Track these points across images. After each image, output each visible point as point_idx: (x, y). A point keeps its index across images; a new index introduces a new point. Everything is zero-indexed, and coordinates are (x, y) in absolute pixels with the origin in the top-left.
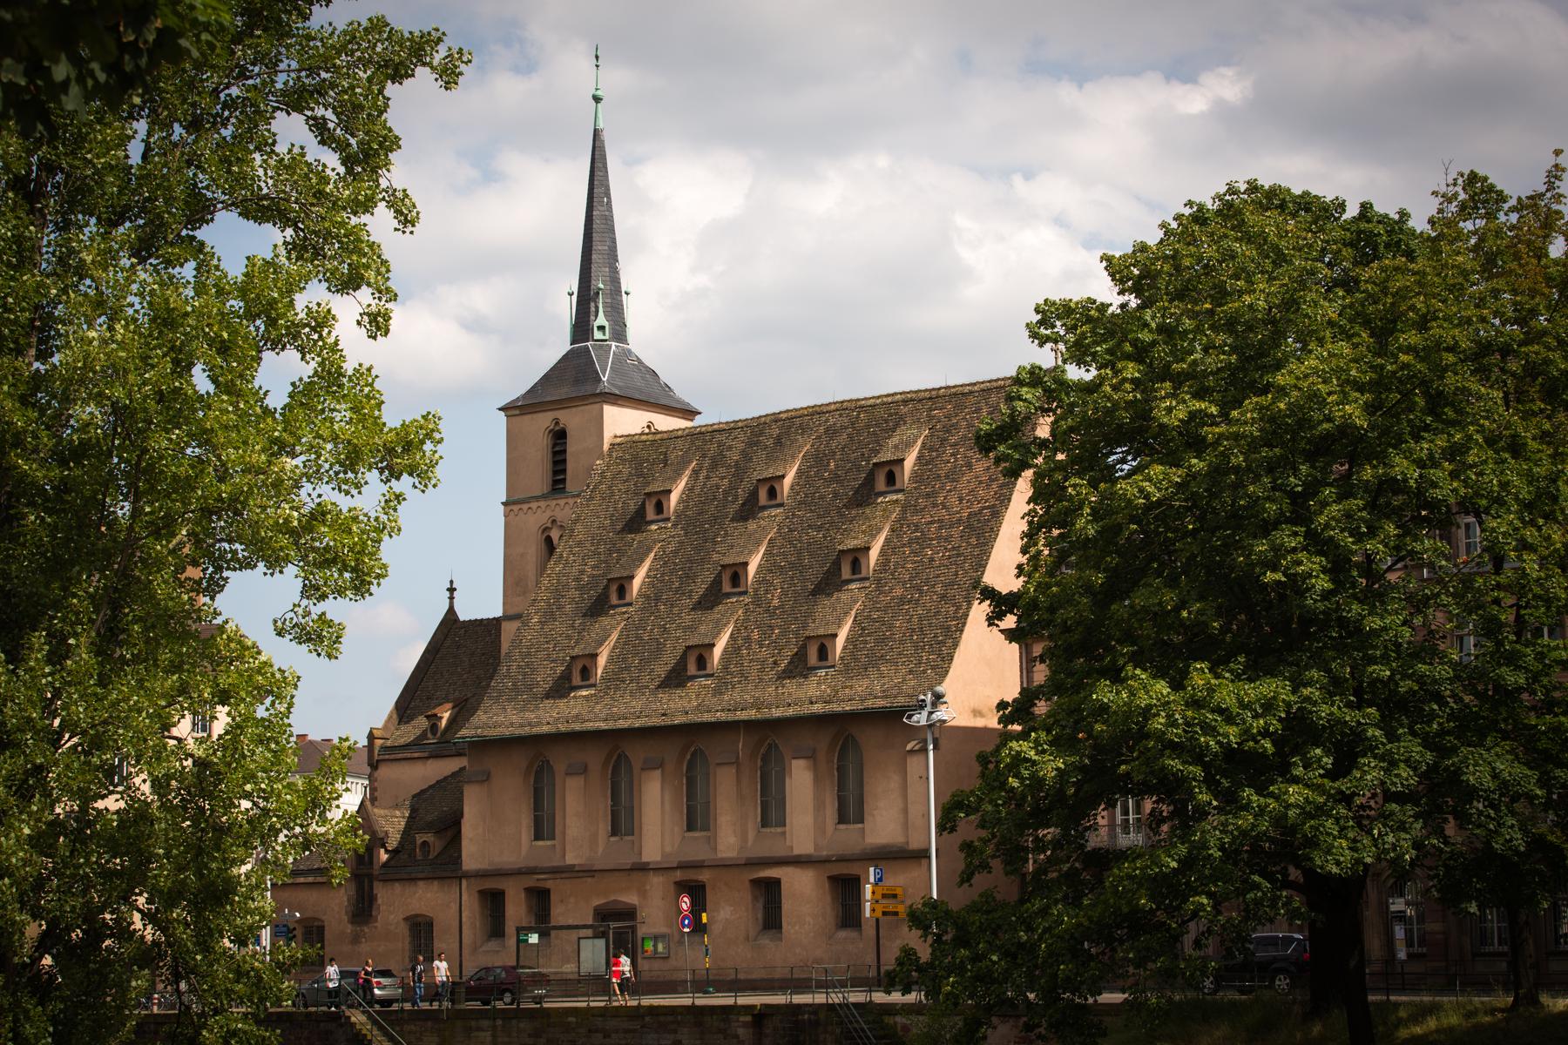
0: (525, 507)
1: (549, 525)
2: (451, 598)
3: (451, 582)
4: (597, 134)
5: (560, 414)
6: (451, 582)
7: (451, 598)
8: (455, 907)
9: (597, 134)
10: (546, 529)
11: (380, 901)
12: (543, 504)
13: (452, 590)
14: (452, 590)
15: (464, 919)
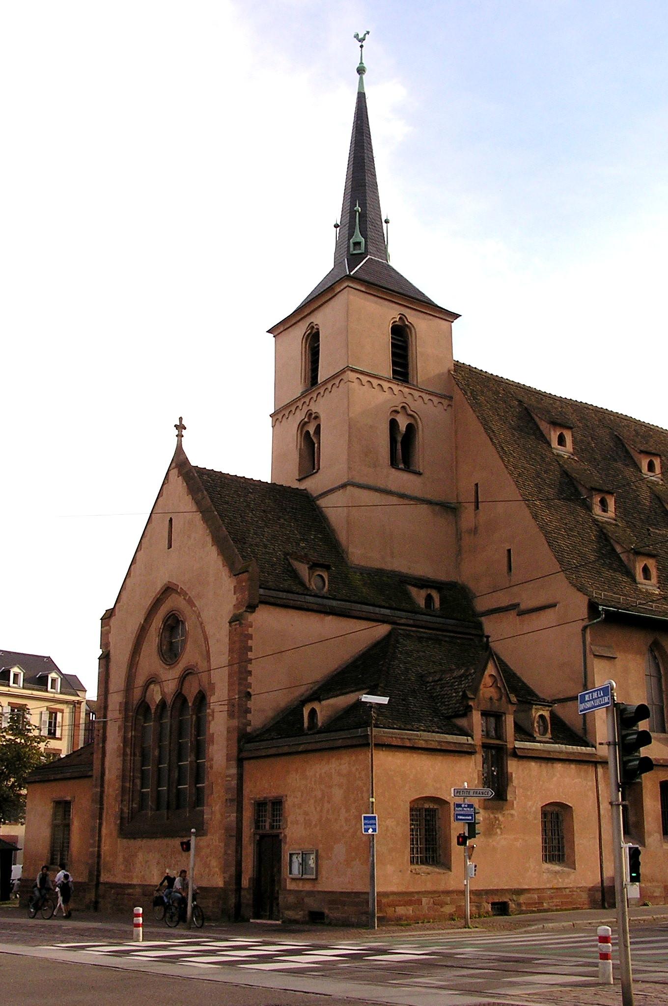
0: (375, 382)
1: (399, 409)
2: (180, 436)
3: (181, 419)
4: (361, 98)
5: (408, 313)
6: (181, 419)
7: (180, 436)
8: (592, 795)
9: (361, 98)
10: (398, 412)
11: (515, 782)
12: (386, 385)
13: (180, 427)
14: (180, 427)
15: (602, 812)
